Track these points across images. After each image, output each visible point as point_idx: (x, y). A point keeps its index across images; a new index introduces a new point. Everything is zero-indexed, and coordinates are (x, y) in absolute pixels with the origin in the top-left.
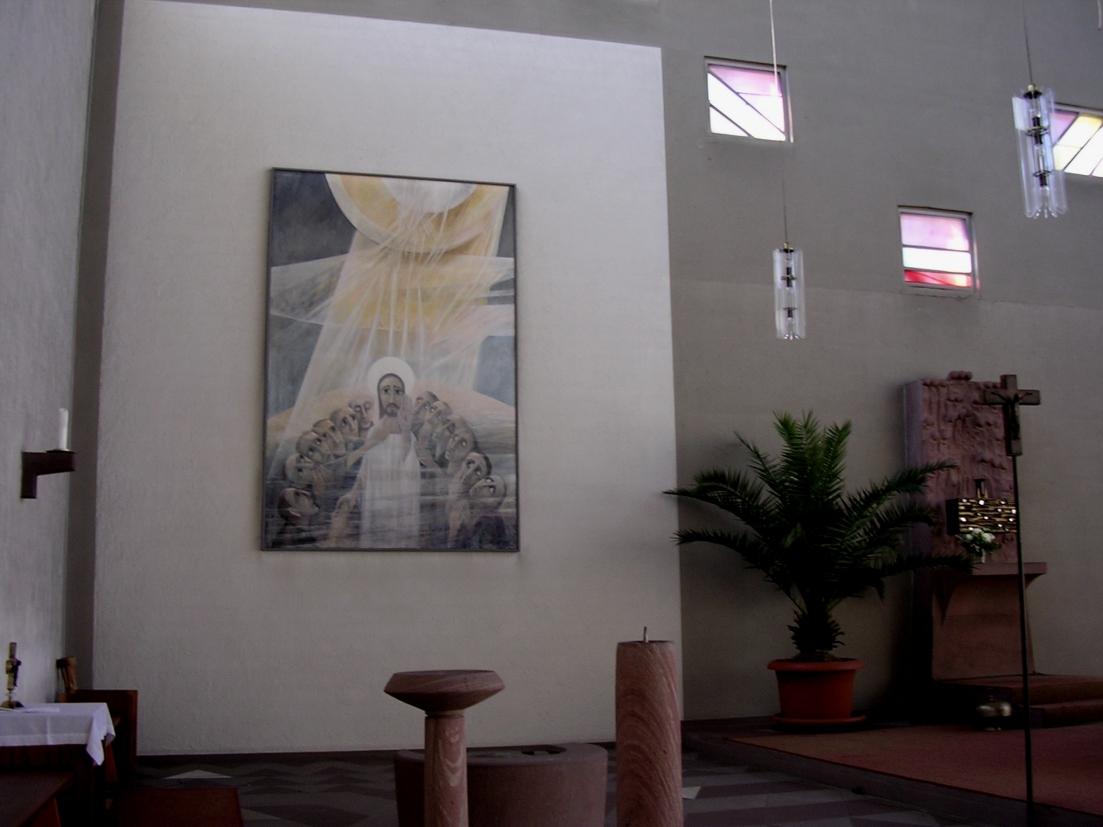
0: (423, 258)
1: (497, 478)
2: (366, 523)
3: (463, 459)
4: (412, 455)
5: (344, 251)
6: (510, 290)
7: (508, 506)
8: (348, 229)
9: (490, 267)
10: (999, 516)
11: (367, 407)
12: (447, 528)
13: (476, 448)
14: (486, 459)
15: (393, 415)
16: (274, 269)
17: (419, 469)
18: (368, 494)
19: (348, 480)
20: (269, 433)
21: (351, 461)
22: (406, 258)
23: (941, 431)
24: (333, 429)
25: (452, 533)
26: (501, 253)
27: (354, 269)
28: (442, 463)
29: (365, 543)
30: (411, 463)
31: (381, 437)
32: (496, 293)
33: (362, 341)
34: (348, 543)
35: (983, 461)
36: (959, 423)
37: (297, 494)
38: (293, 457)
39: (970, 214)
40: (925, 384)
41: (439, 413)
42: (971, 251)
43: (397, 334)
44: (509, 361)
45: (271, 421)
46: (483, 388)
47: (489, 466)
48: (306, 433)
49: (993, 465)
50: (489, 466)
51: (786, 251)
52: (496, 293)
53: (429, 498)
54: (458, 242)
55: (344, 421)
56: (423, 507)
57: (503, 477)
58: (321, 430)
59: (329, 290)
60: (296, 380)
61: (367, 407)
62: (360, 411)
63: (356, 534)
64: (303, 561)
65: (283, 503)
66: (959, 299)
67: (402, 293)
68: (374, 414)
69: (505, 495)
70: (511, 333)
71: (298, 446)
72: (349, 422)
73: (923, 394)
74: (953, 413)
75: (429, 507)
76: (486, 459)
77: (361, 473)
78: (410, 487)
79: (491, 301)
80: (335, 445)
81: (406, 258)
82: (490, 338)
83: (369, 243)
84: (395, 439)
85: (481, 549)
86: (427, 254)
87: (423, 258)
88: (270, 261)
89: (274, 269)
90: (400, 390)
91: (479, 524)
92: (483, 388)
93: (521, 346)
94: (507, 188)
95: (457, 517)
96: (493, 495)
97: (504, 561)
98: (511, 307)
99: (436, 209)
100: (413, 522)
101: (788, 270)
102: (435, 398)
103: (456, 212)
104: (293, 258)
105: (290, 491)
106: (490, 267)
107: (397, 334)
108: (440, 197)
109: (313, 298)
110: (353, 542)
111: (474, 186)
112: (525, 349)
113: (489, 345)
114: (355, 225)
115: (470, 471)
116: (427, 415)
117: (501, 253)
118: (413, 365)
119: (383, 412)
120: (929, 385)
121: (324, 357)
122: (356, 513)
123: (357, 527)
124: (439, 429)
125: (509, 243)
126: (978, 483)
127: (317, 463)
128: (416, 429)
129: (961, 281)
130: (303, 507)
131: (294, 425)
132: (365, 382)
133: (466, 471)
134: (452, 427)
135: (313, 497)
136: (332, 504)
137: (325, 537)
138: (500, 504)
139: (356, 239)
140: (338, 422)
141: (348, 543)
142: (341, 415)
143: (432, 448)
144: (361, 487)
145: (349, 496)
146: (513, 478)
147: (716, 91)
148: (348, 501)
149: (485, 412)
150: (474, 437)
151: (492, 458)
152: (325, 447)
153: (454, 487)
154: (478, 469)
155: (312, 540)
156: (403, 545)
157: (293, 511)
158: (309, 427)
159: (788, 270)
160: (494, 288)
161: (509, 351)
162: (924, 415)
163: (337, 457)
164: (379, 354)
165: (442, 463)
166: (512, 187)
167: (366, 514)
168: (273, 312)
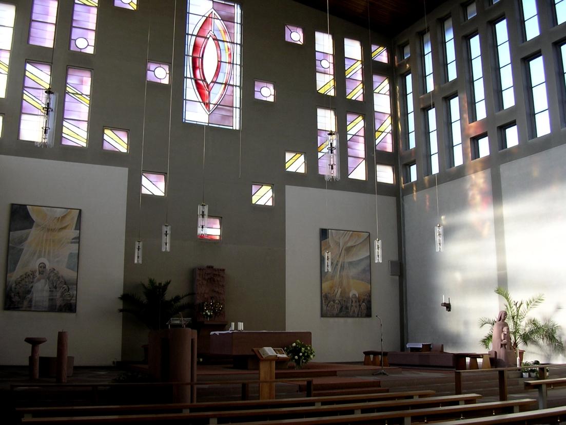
0: (53, 230)
1: (71, 292)
2: (33, 304)
3: (61, 287)
4: (47, 285)
5: (31, 228)
6: (78, 240)
7: (74, 300)
8: (33, 222)
9: (73, 233)
10: (216, 307)
11: (35, 271)
12: (56, 306)
13: (65, 283)
14: (68, 287)
15: (42, 274)
16: (11, 233)
17: (49, 289)
18: (34, 295)
19: (29, 292)
20: (8, 278)
21: (30, 287)
22: (48, 230)
23: (202, 283)
24: (25, 277)
25: (57, 307)
26: (76, 229)
27: (34, 233)
28: (56, 288)
29: (33, 309)
30: (47, 287)
31: (39, 280)
32: (73, 241)
33: (35, 254)
34: (28, 309)
35: (215, 291)
36: (209, 281)
37: (14, 295)
38: (14, 285)
39: (221, 217)
40: (198, 269)
41: (55, 274)
42: (220, 229)
43: (45, 252)
44: (76, 260)
45: (8, 275)
46: (69, 267)
47: (69, 289)
48: (18, 278)
49: (218, 293)
50: (69, 289)
51: (203, 205)
52: (73, 241)
53: (51, 297)
54: (63, 226)
55: (29, 275)
56: (49, 299)
57: (73, 292)
58: (22, 278)
59: (26, 239)
60: (16, 263)
61: (35, 271)
62: (33, 273)
63: (30, 307)
64: (15, 314)
65: (11, 298)
66: (215, 243)
67: (46, 240)
68: (37, 274)
69: (73, 297)
70: (77, 252)
71: (15, 282)
72: (30, 276)
73: (198, 272)
74: (207, 278)
75: (51, 300)
76: (68, 287)
77: (33, 290)
78: (46, 294)
79: (72, 243)
80: (26, 282)
81: (48, 230)
82: (71, 253)
83: (38, 226)
84: (43, 281)
85: (65, 312)
86: (54, 229)
87: (53, 230)
88: (10, 230)
89: (11, 233)
90: (45, 267)
91: (65, 305)
92: (69, 267)
93: (79, 255)
94: (79, 211)
95: (59, 302)
96: (69, 297)
97: (72, 315)
98: (78, 245)
99: (58, 217)
100: (46, 304)
101: (139, 247)
102: (55, 270)
103: (64, 217)
104: (16, 230)
105: (13, 294)
106: (73, 233)
107: (45, 252)
108: (59, 213)
109: (22, 241)
110: (29, 308)
111: (69, 210)
112: (81, 256)
113: (71, 255)
114: (34, 220)
115: (63, 290)
116: (52, 274)
117: (76, 229)
118: (49, 261)
119: (40, 273)
120: (200, 269)
121: (24, 258)
122: (31, 301)
123: (31, 305)
124: (55, 279)
125: (78, 226)
126: (212, 298)
127: (21, 287)
128: (48, 278)
129: (218, 238)
130: (16, 299)
131: (15, 276)
132: (35, 265)
133: (62, 290)
134: (59, 278)
135: (19, 296)
136: (24, 298)
137: (22, 307)
138: (71, 300)
139: (35, 224)
140: (27, 275)
141: (28, 309)
142: (28, 274)
143: (53, 283)
144: (32, 294)
145: (29, 296)
146: (75, 292)
147: (144, 181)
148: (28, 298)
149: (68, 274)
150: (65, 281)
151: (70, 287)
152: (23, 282)
153: (59, 294)
154: (65, 290)
155: (18, 308)
156: (43, 310)
157: (14, 300)
158: (19, 277)
159: (139, 247)
160: (73, 239)
161: (76, 256)
162: (198, 278)
163: (26, 285)
164: (39, 257)
165: (56, 288)
166: (80, 211)
167: (33, 302)
168: (10, 245)
